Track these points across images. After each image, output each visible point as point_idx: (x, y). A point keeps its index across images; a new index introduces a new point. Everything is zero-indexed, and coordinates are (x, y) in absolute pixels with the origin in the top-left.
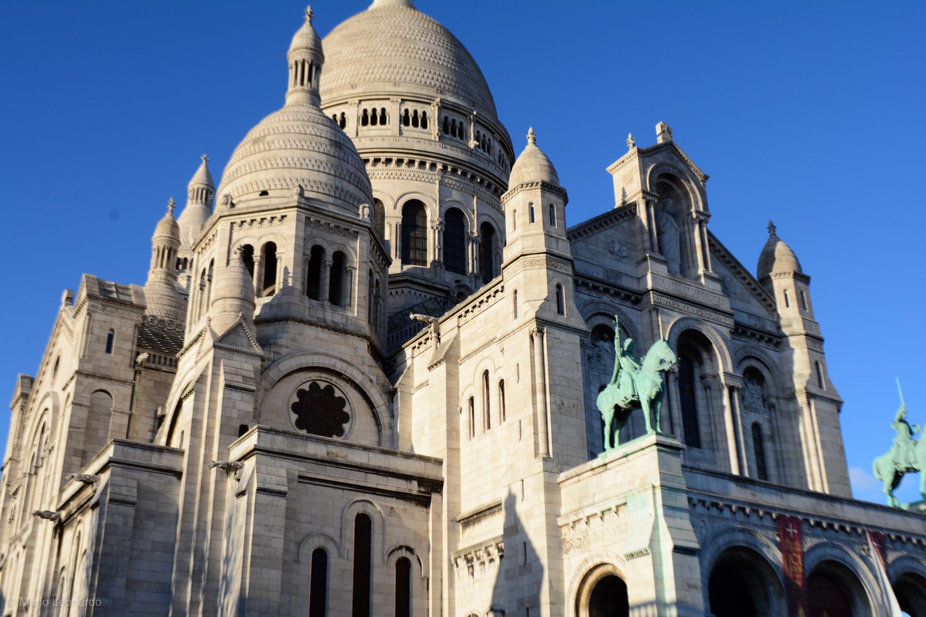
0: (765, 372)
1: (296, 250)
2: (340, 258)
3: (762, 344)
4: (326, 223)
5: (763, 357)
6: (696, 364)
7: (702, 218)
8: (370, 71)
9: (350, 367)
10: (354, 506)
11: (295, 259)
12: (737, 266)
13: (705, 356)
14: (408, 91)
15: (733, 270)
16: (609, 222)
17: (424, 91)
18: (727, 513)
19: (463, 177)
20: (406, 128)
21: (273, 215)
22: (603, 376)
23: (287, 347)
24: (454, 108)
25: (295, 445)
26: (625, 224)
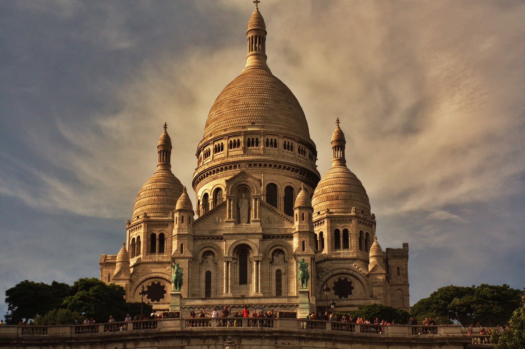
0: (284, 250)
1: (144, 238)
2: (162, 236)
6: (248, 255)
9: (164, 275)
11: (143, 241)
13: (250, 251)
14: (230, 132)
17: (237, 130)
19: (255, 166)
20: (231, 150)
21: (137, 226)
22: (207, 268)
23: (141, 273)
24: (253, 133)
26: (222, 210)
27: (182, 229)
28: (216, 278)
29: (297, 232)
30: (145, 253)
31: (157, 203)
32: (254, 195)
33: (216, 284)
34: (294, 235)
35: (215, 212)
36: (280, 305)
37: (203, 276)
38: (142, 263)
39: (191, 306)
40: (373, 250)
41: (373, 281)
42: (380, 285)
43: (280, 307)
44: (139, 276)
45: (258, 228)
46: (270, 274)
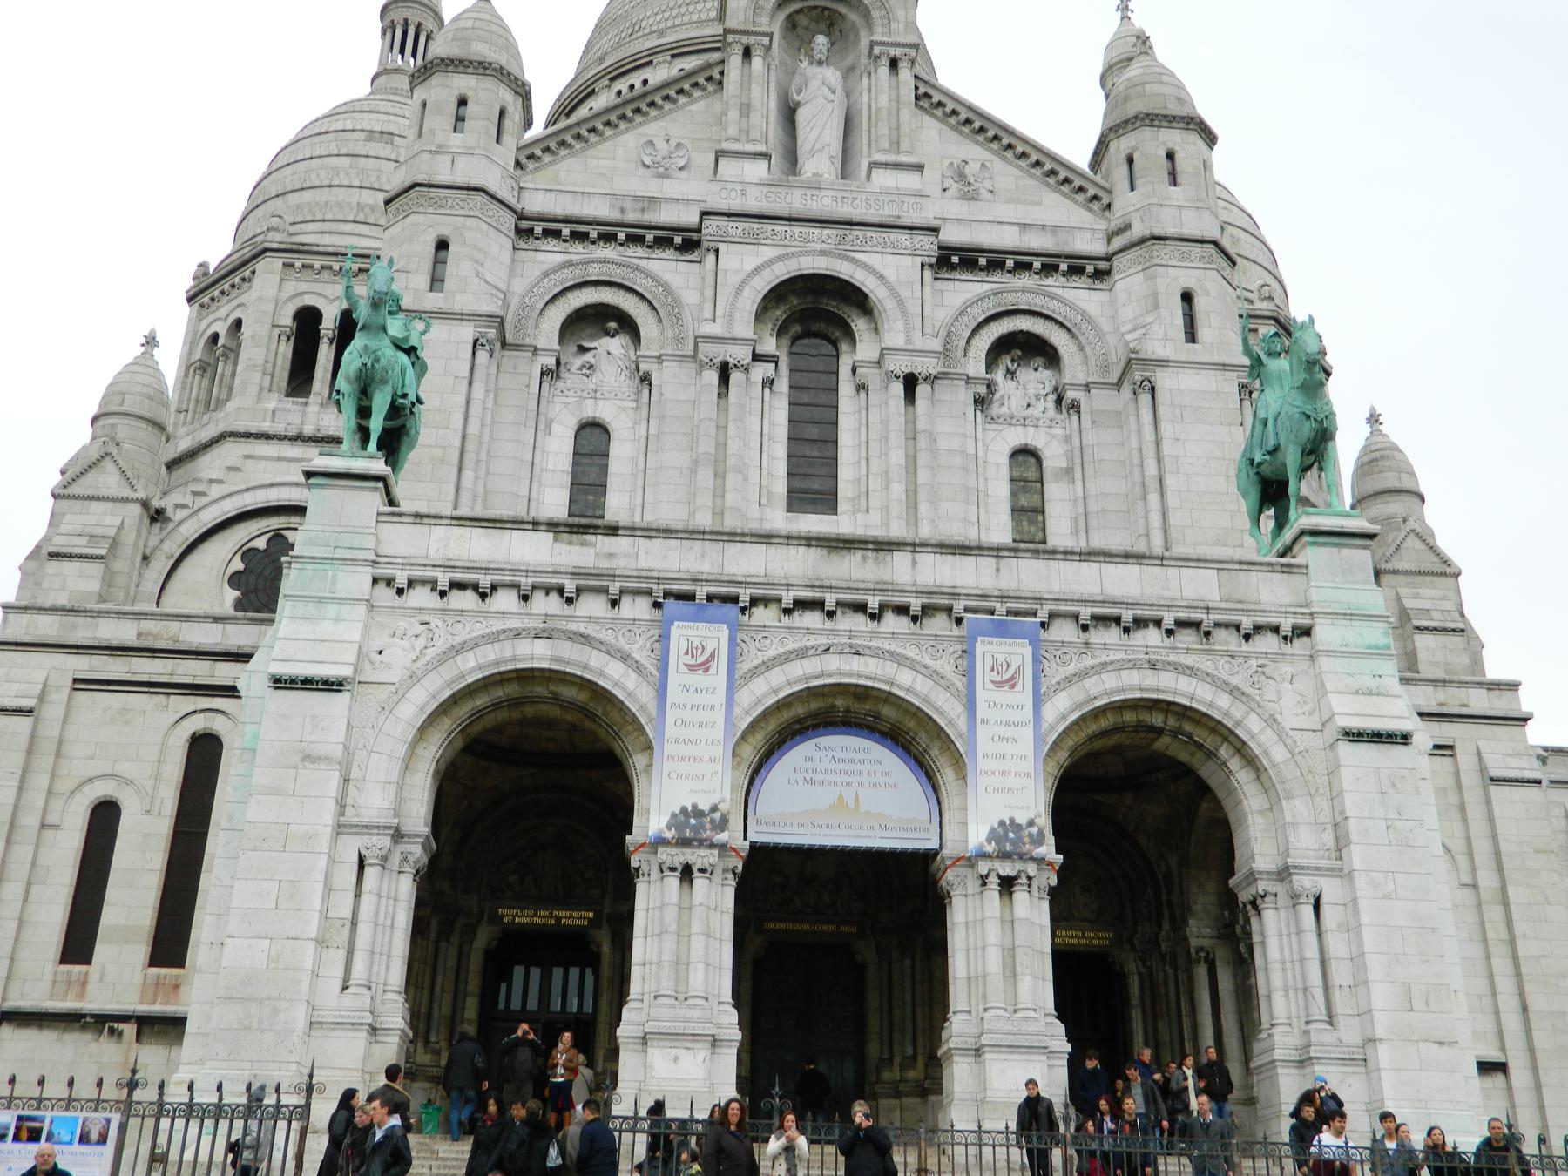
0: (1057, 337)
3: (1053, 282)
4: (322, 267)
5: (1050, 307)
6: (844, 347)
7: (893, 52)
8: (637, 28)
10: (185, 722)
12: (1001, 134)
13: (859, 325)
15: (995, 146)
16: (644, 107)
18: (505, 601)
22: (589, 402)
23: (220, 482)
25: (74, 627)
26: (694, 107)
27: (448, 158)
28: (642, 458)
29: (1142, 241)
30: (253, 390)
31: (345, 182)
32: (885, 39)
33: (639, 500)
34: (1119, 262)
35: (653, 112)
36: (1168, 620)
37: (559, 449)
38: (234, 435)
39: (459, 576)
40: (1380, 463)
41: (1408, 603)
42: (1453, 626)
43: (1169, 632)
44: (204, 494)
45: (912, 200)
46: (977, 465)
